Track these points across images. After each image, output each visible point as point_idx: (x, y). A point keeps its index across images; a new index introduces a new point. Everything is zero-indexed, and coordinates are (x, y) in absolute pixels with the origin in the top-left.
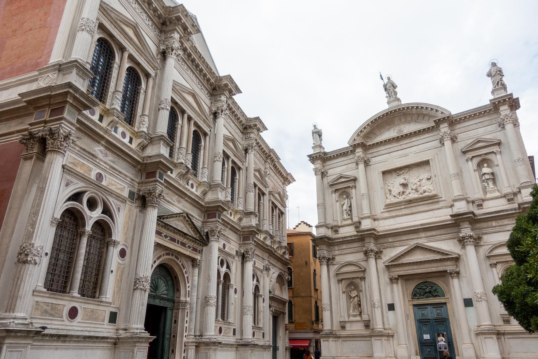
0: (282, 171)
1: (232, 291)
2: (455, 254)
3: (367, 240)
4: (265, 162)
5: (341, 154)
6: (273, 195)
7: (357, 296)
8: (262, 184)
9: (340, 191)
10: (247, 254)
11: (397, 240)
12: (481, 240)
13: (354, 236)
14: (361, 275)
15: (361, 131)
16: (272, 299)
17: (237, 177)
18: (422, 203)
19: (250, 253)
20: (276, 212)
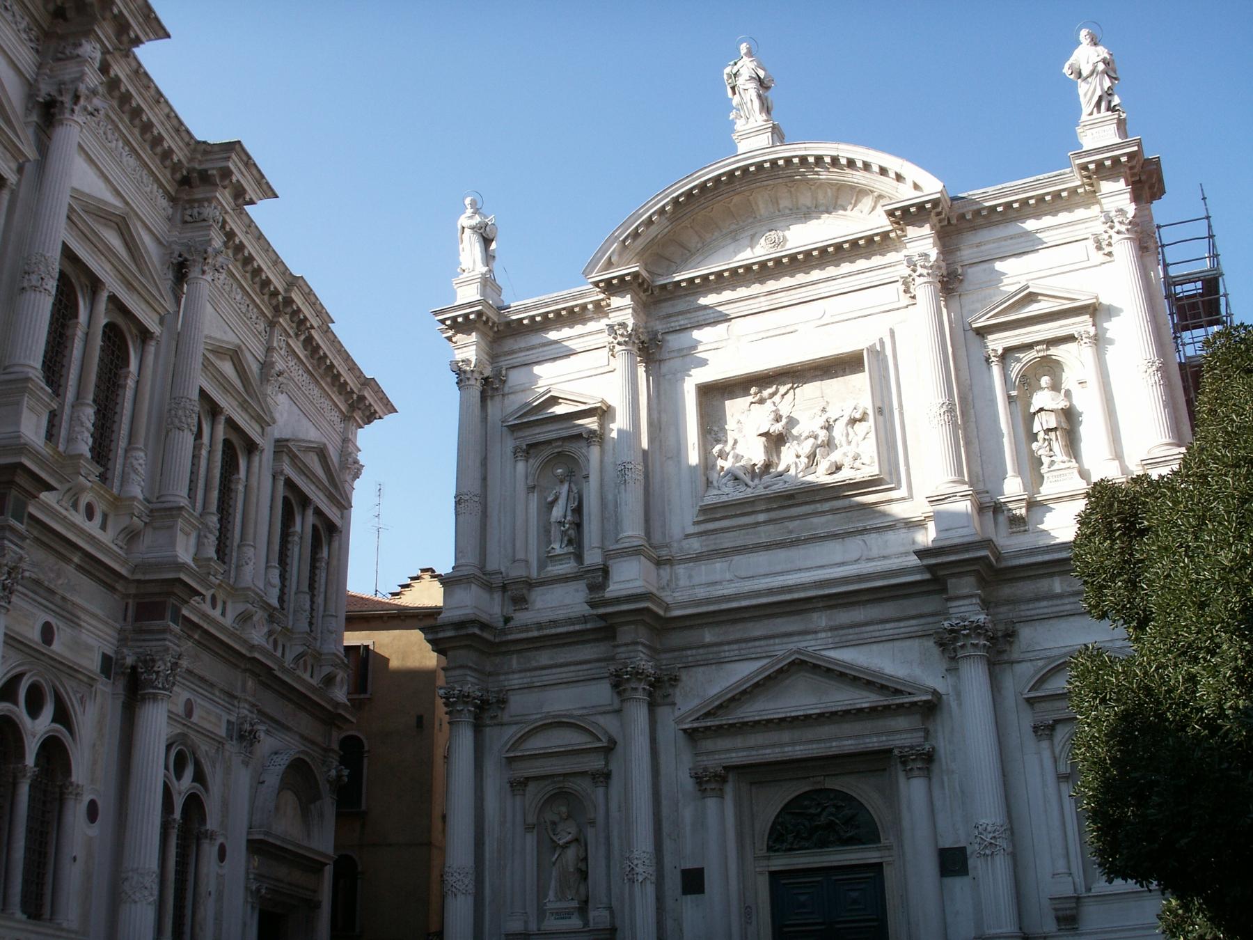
0: (341, 368)
1: (76, 813)
2: (925, 690)
3: (626, 634)
4: (272, 324)
6: (294, 458)
7: (577, 840)
8: (244, 405)
9: (547, 452)
10: (150, 672)
11: (732, 637)
12: (1011, 643)
13: (585, 619)
14: (596, 763)
15: (636, 235)
16: (256, 847)
17: (133, 366)
18: (827, 506)
19: (159, 666)
20: (303, 525)
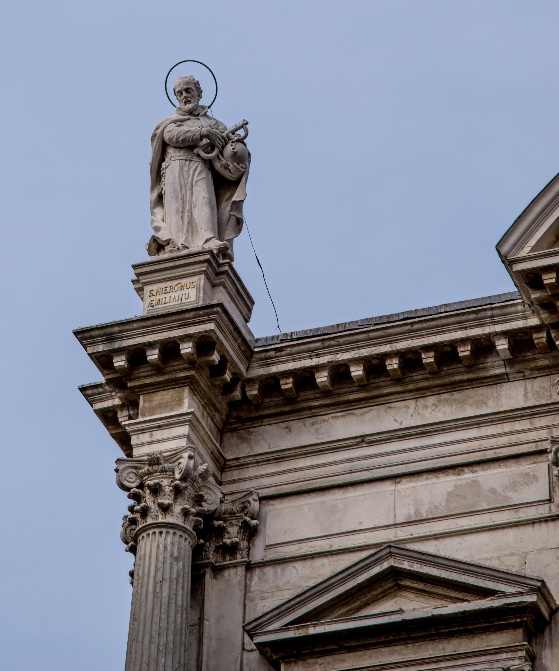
5: (410, 360)
